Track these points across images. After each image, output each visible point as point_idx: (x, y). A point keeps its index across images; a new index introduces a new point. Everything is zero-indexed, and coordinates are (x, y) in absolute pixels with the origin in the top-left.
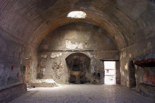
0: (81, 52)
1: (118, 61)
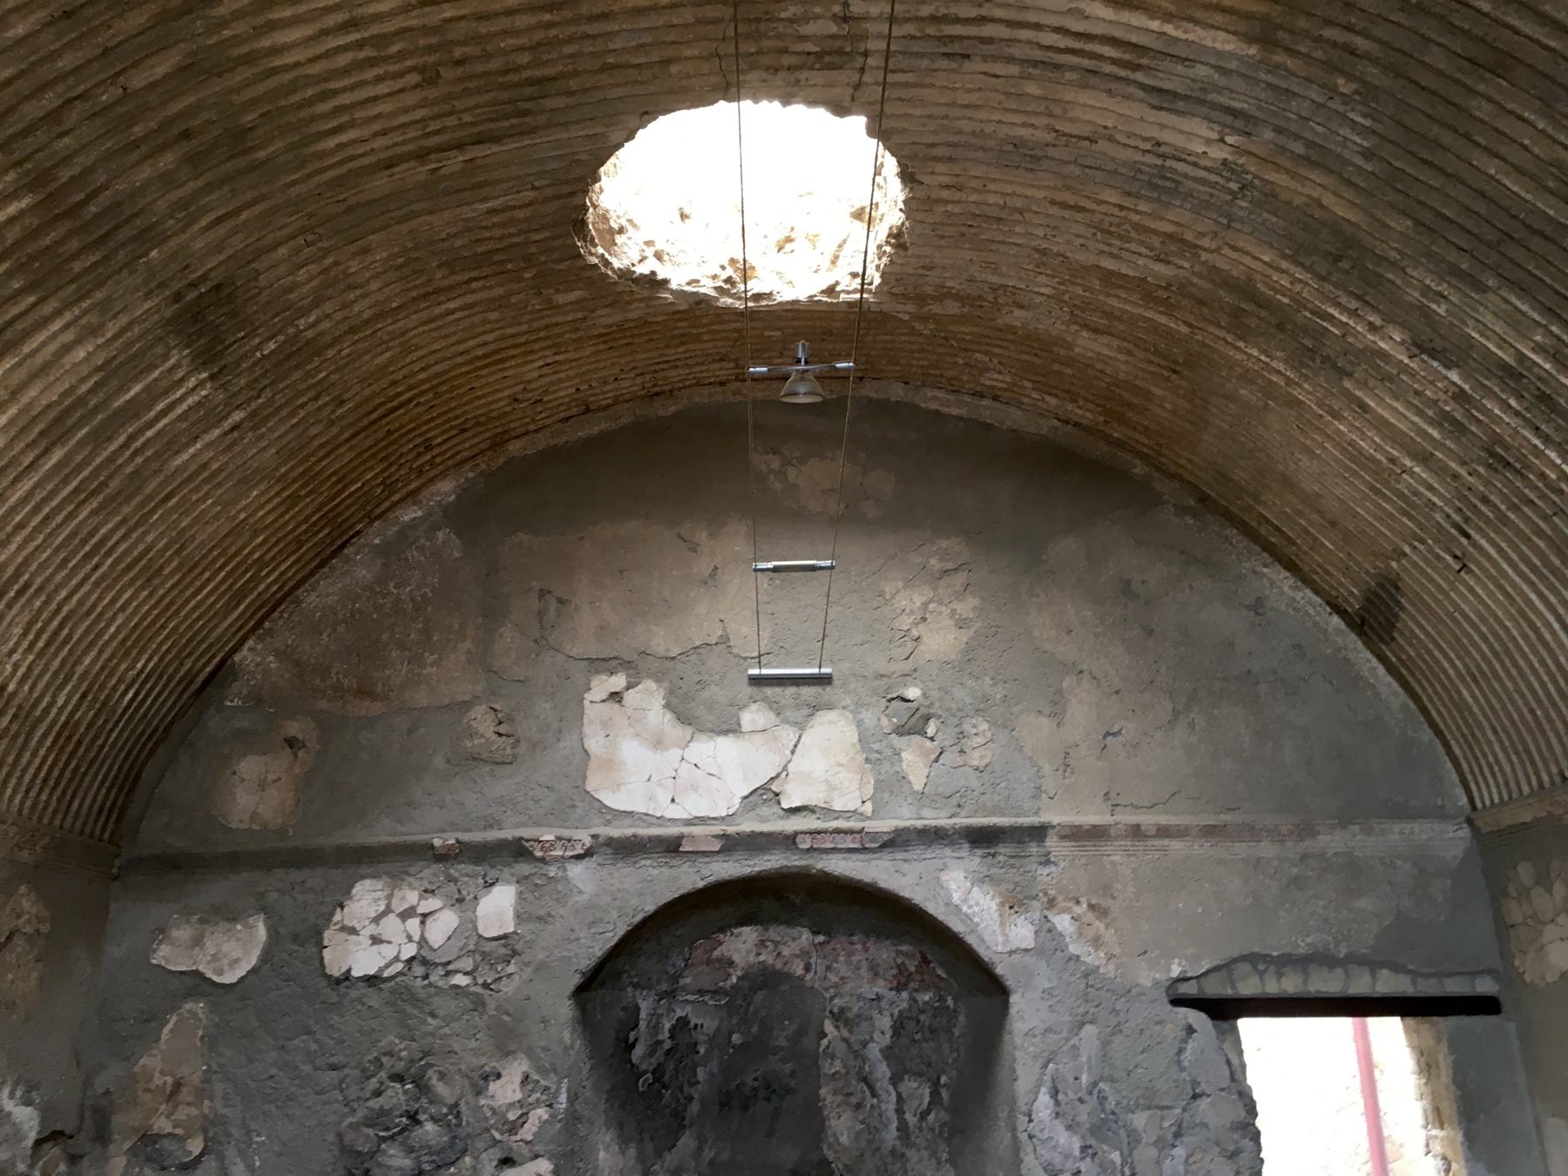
0: (839, 866)
1: (1487, 1006)
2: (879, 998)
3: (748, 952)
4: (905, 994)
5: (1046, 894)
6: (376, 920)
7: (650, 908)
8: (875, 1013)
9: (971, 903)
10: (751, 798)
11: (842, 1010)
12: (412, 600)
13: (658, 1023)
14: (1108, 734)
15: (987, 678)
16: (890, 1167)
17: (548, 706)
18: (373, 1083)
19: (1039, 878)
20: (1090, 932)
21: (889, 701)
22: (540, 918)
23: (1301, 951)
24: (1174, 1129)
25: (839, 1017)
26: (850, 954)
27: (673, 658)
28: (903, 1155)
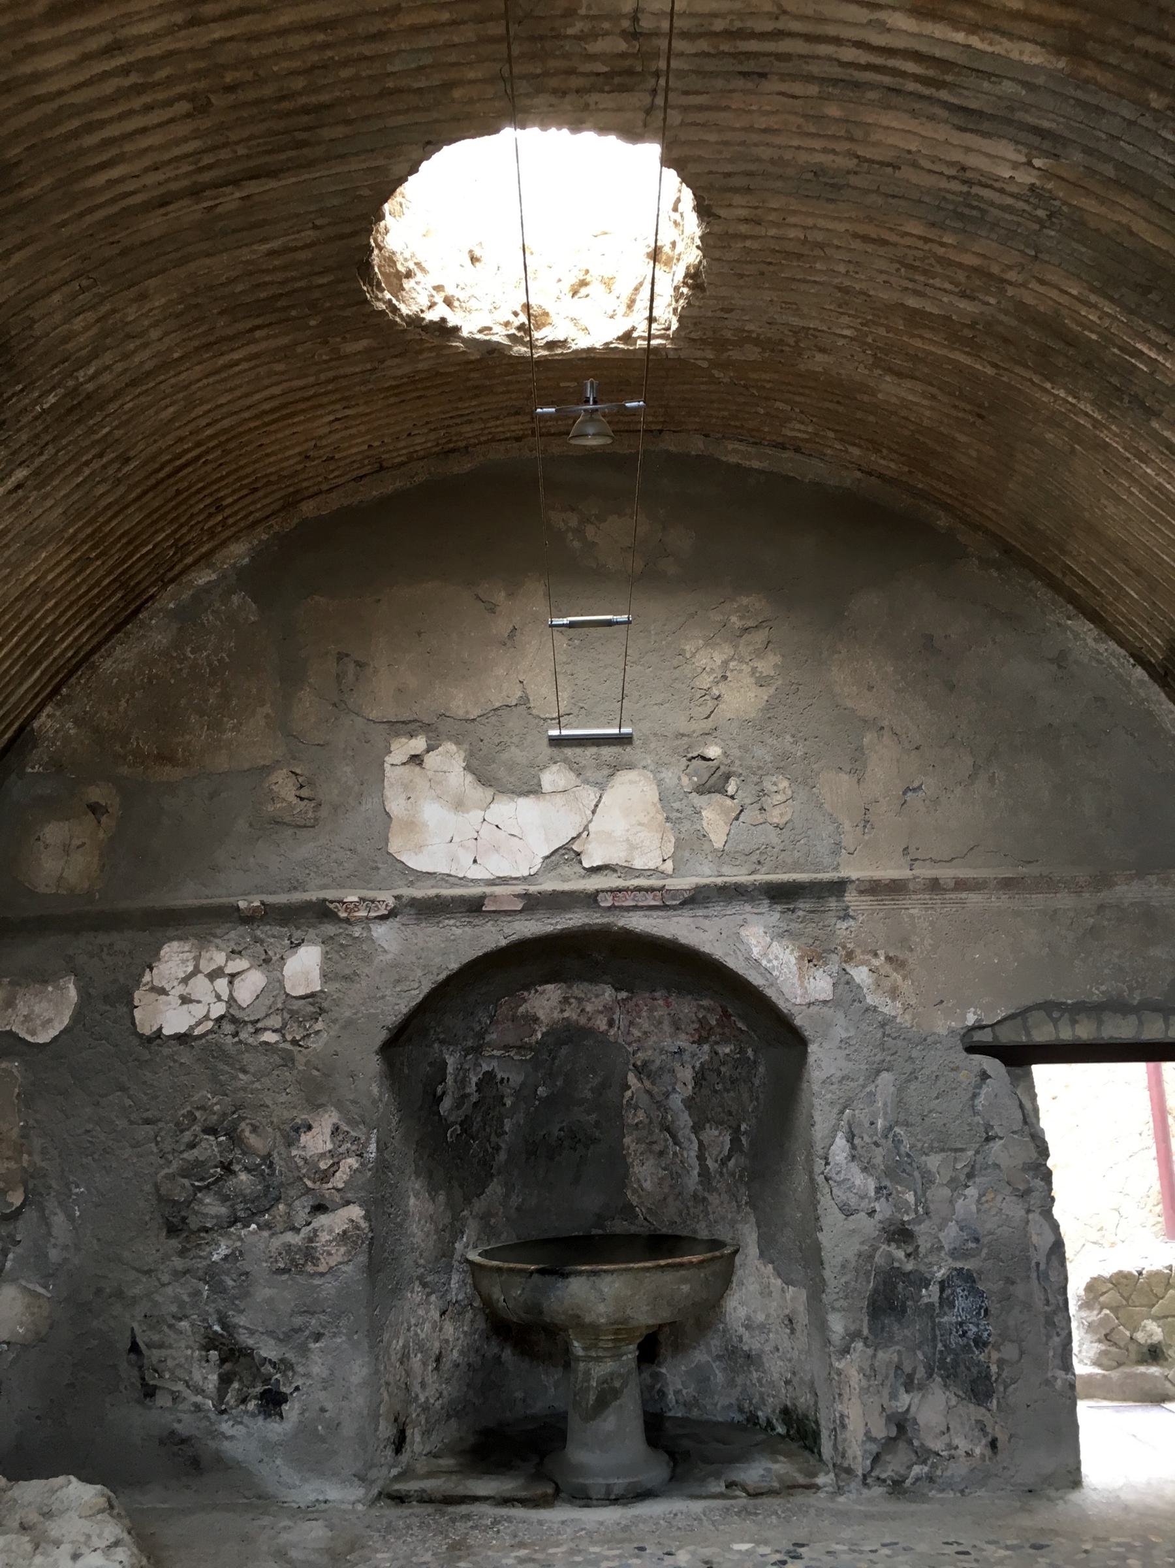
0: (640, 923)
2: (681, 1051)
3: (551, 1009)
4: (706, 1047)
5: (844, 947)
6: (185, 980)
7: (454, 966)
8: (677, 1066)
9: (771, 957)
10: (553, 858)
11: (645, 1063)
12: (210, 665)
13: (465, 1077)
14: (908, 790)
15: (788, 737)
16: (692, 1210)
17: (348, 769)
18: (187, 1137)
19: (838, 932)
20: (887, 984)
21: (690, 760)
22: (346, 978)
23: (1095, 998)
24: (967, 1170)
25: (642, 1070)
26: (651, 1010)
27: (474, 720)
28: (704, 1199)
